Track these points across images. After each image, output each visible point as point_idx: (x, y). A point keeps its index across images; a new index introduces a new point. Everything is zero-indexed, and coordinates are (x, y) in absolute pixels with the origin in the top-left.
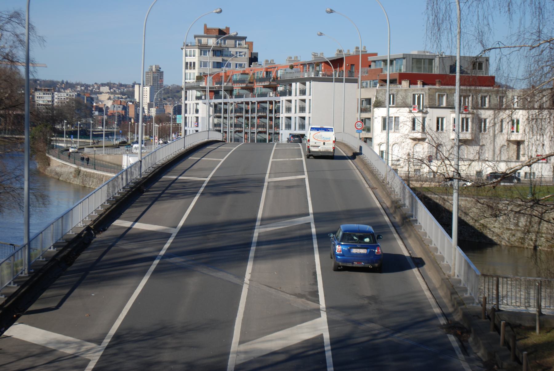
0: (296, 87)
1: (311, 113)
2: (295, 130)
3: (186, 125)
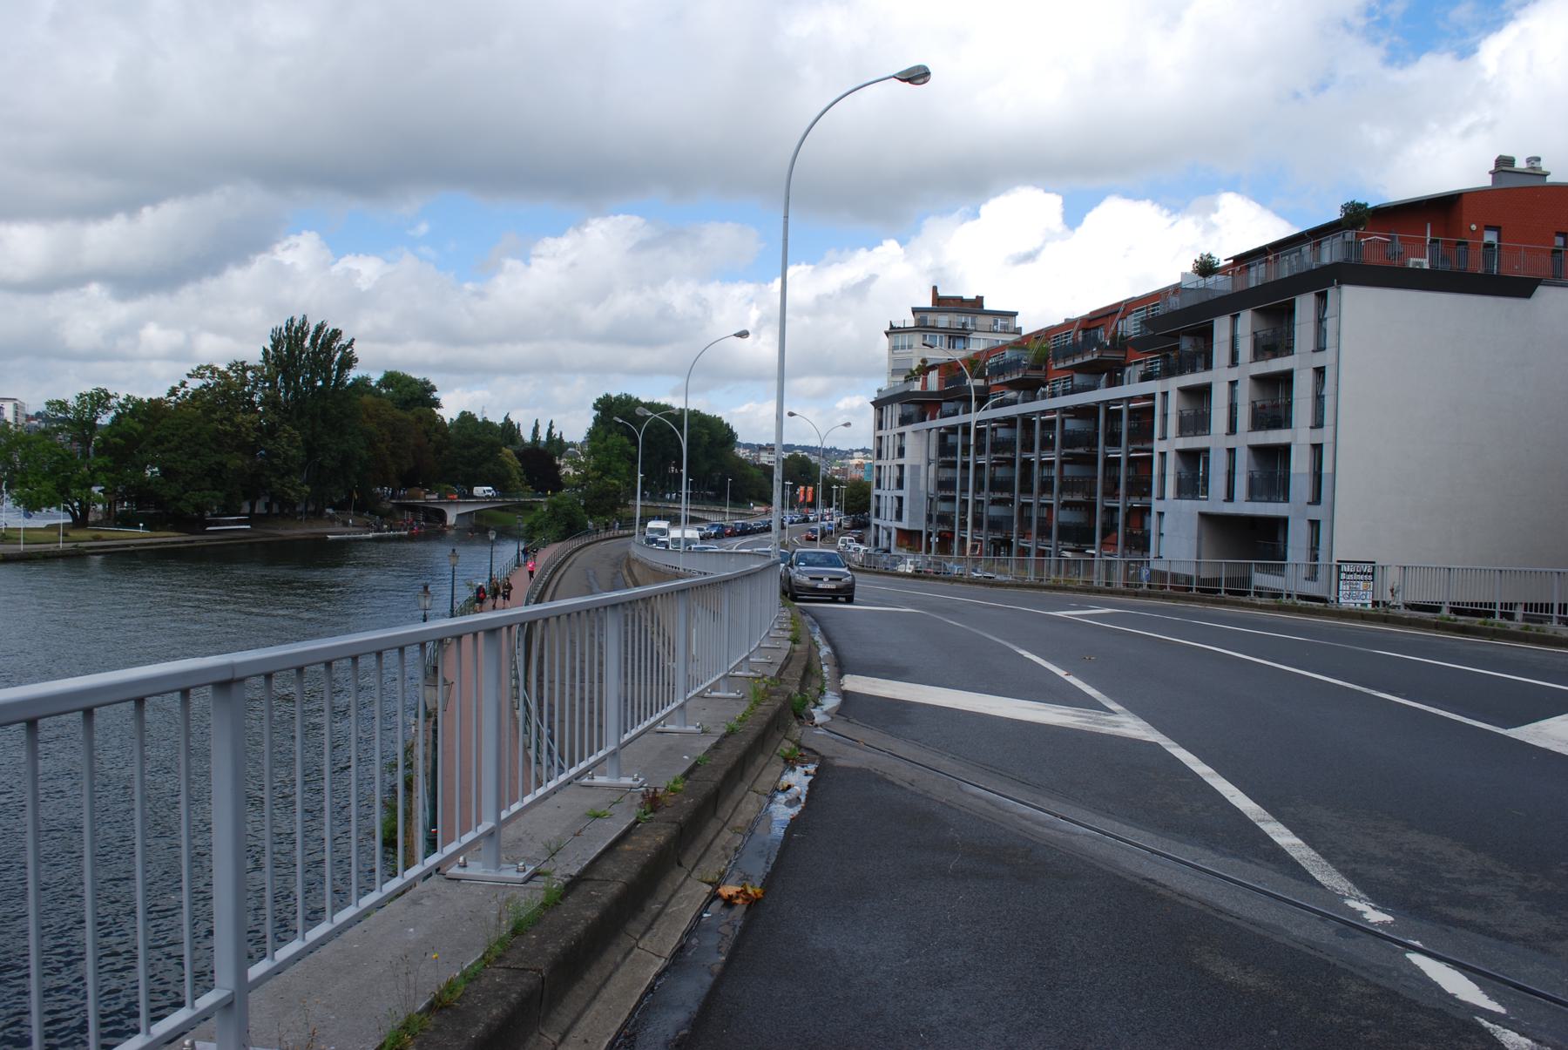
2: (1230, 497)
3: (879, 486)
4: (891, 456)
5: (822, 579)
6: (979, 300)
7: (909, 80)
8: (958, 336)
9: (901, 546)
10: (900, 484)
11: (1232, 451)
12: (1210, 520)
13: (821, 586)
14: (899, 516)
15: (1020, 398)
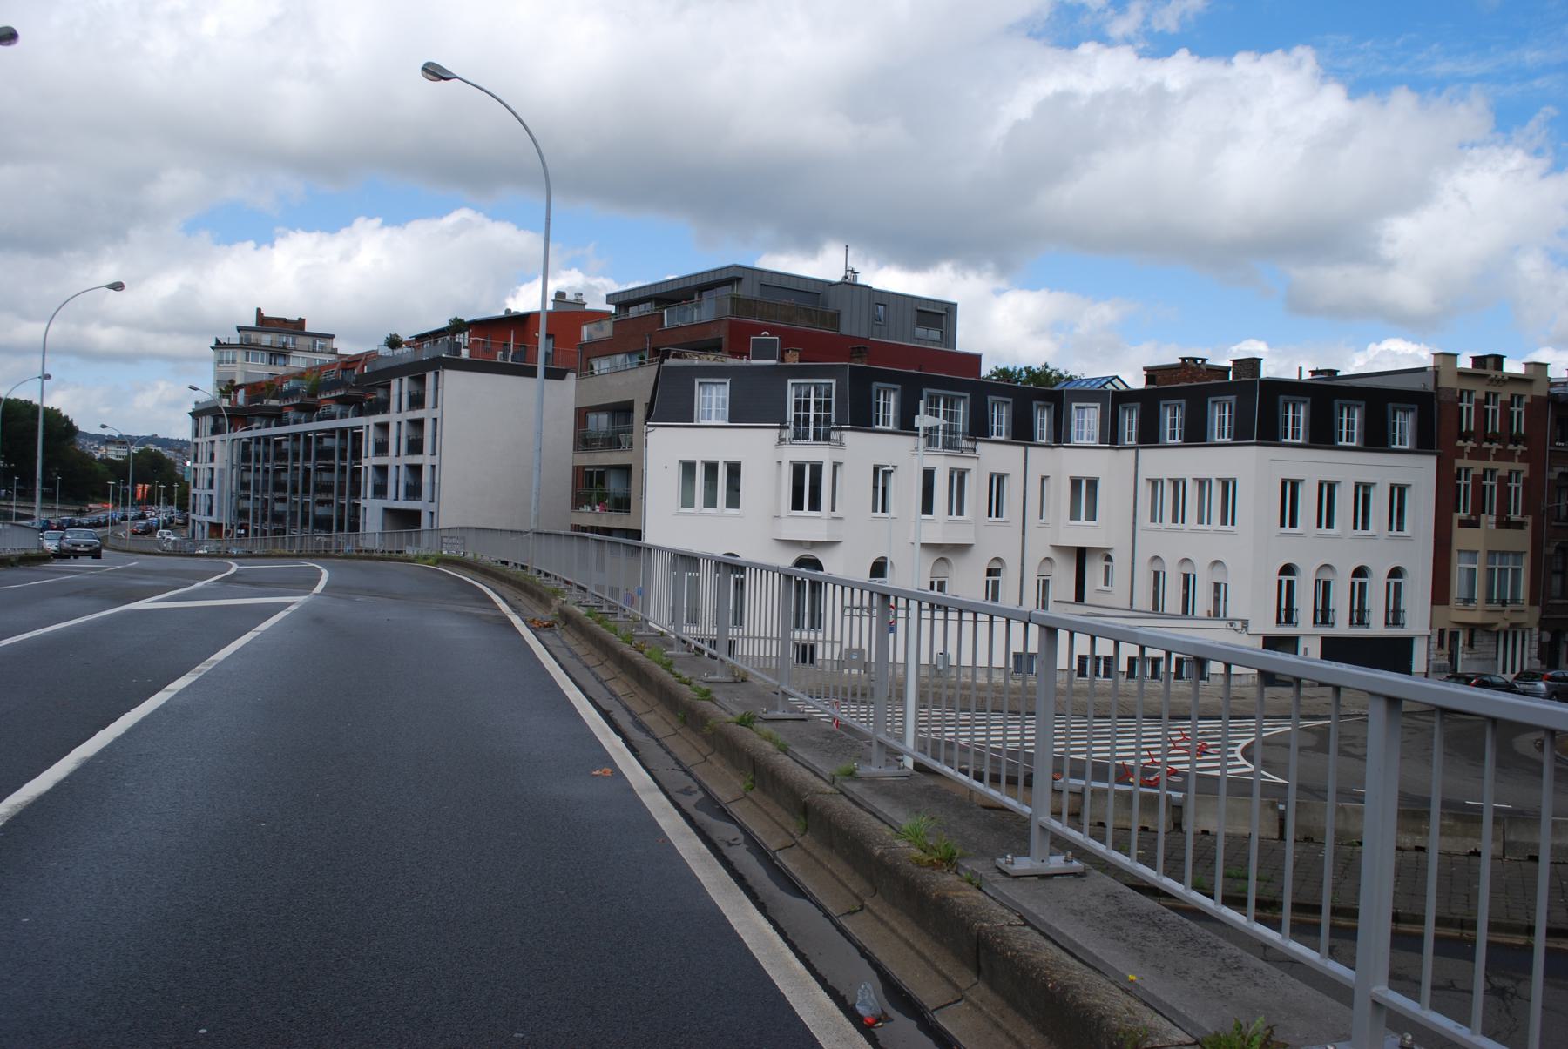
0: (400, 388)
1: (438, 456)
4: (204, 460)
5: (79, 546)
6: (302, 322)
7: (114, 289)
8: (278, 354)
9: (213, 537)
10: (211, 485)
11: (398, 467)
12: (389, 512)
13: (79, 549)
14: (210, 513)
15: (303, 418)
